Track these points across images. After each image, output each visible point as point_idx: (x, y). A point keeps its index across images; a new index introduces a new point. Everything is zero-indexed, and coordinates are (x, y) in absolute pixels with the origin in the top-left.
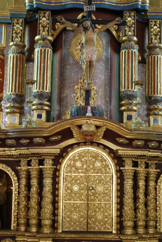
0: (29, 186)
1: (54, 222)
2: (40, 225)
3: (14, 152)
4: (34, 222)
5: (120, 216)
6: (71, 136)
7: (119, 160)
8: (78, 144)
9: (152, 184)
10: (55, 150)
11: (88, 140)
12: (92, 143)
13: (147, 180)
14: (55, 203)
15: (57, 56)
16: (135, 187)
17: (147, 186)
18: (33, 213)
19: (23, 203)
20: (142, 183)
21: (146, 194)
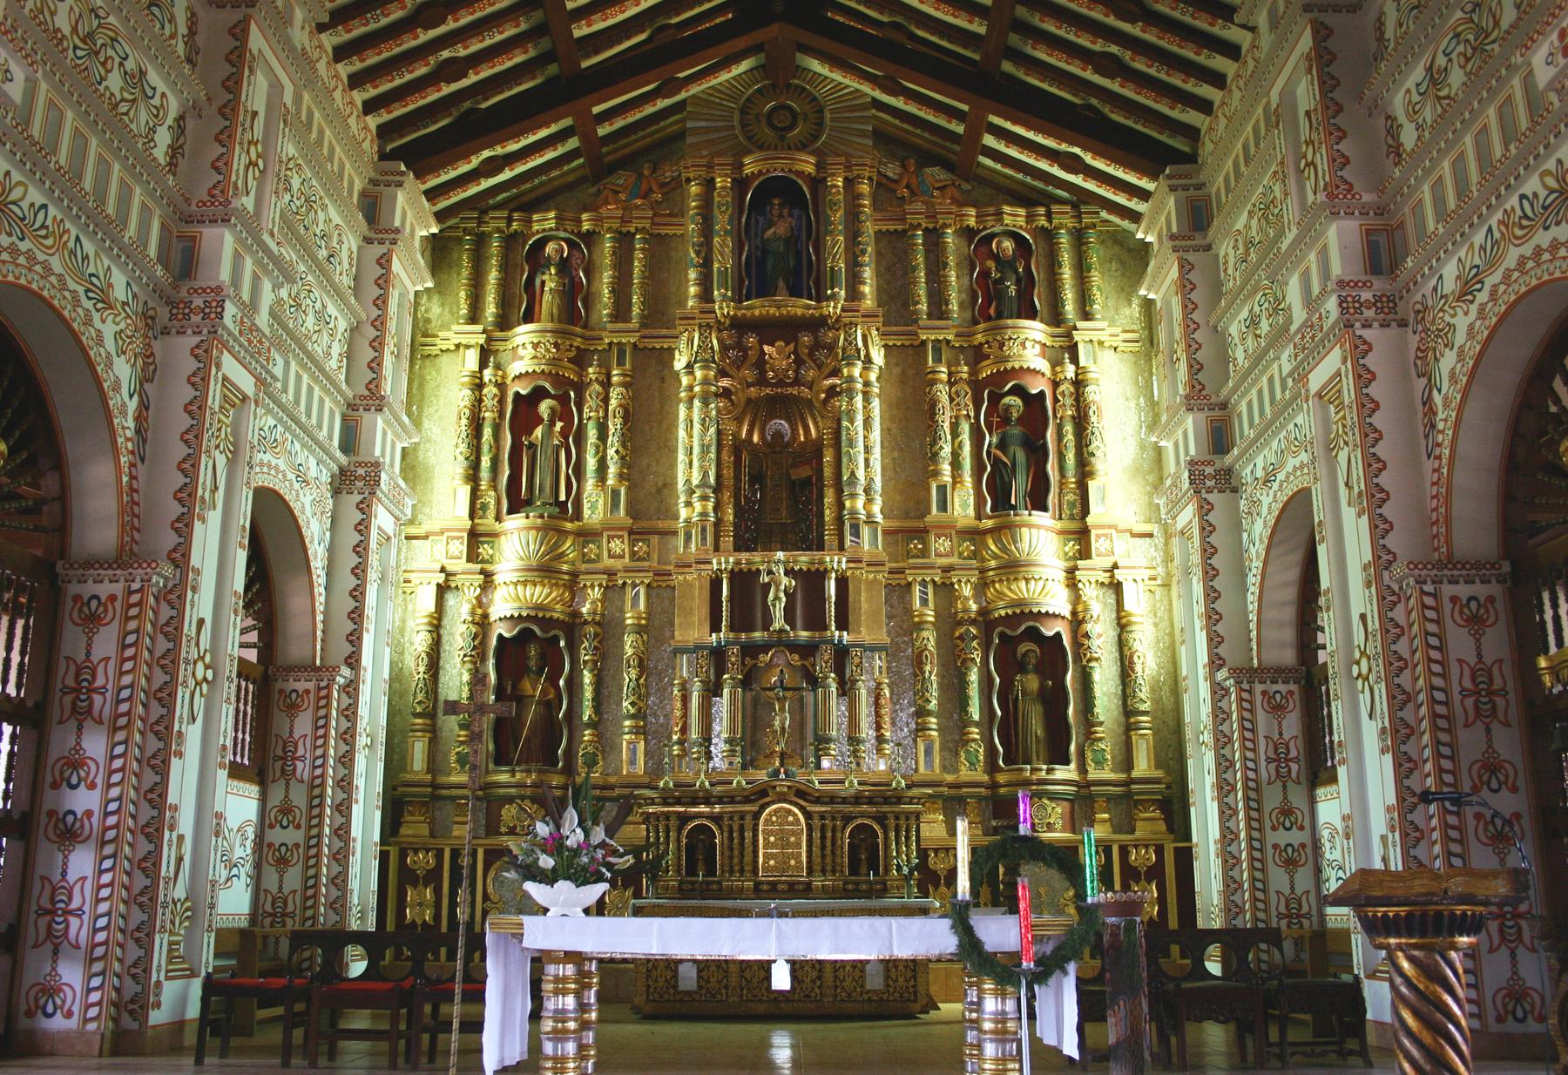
0: (731, 839)
1: (755, 871)
2: (742, 871)
3: (717, 809)
4: (737, 868)
5: (809, 862)
6: (767, 795)
7: (808, 816)
8: (774, 802)
9: (839, 835)
10: (755, 808)
11: (782, 798)
12: (785, 801)
13: (834, 831)
14: (755, 852)
15: (749, 694)
16: (823, 838)
17: (834, 836)
18: (736, 861)
19: (727, 853)
20: (829, 834)
21: (834, 843)
